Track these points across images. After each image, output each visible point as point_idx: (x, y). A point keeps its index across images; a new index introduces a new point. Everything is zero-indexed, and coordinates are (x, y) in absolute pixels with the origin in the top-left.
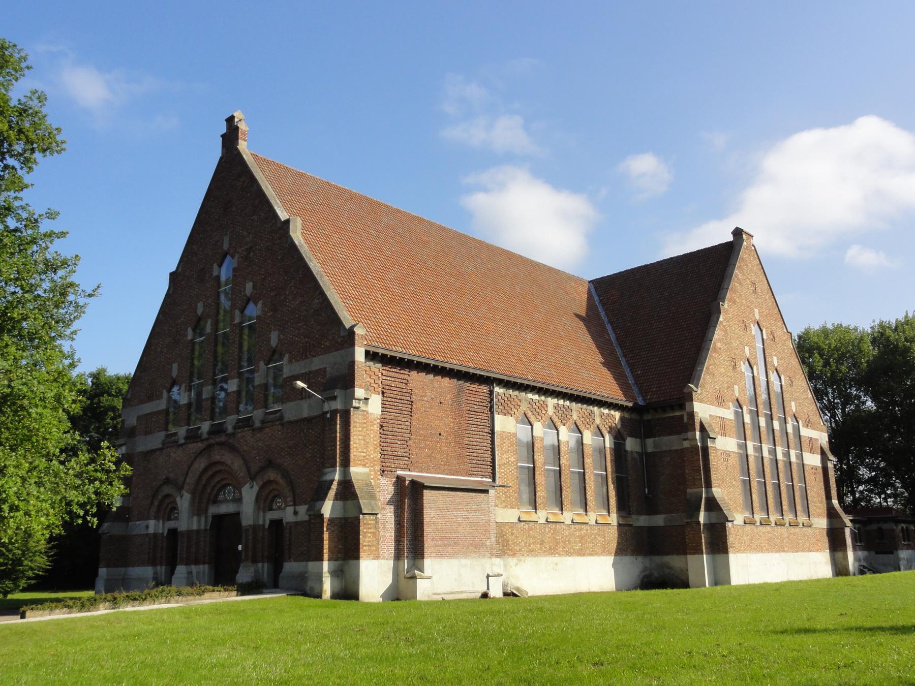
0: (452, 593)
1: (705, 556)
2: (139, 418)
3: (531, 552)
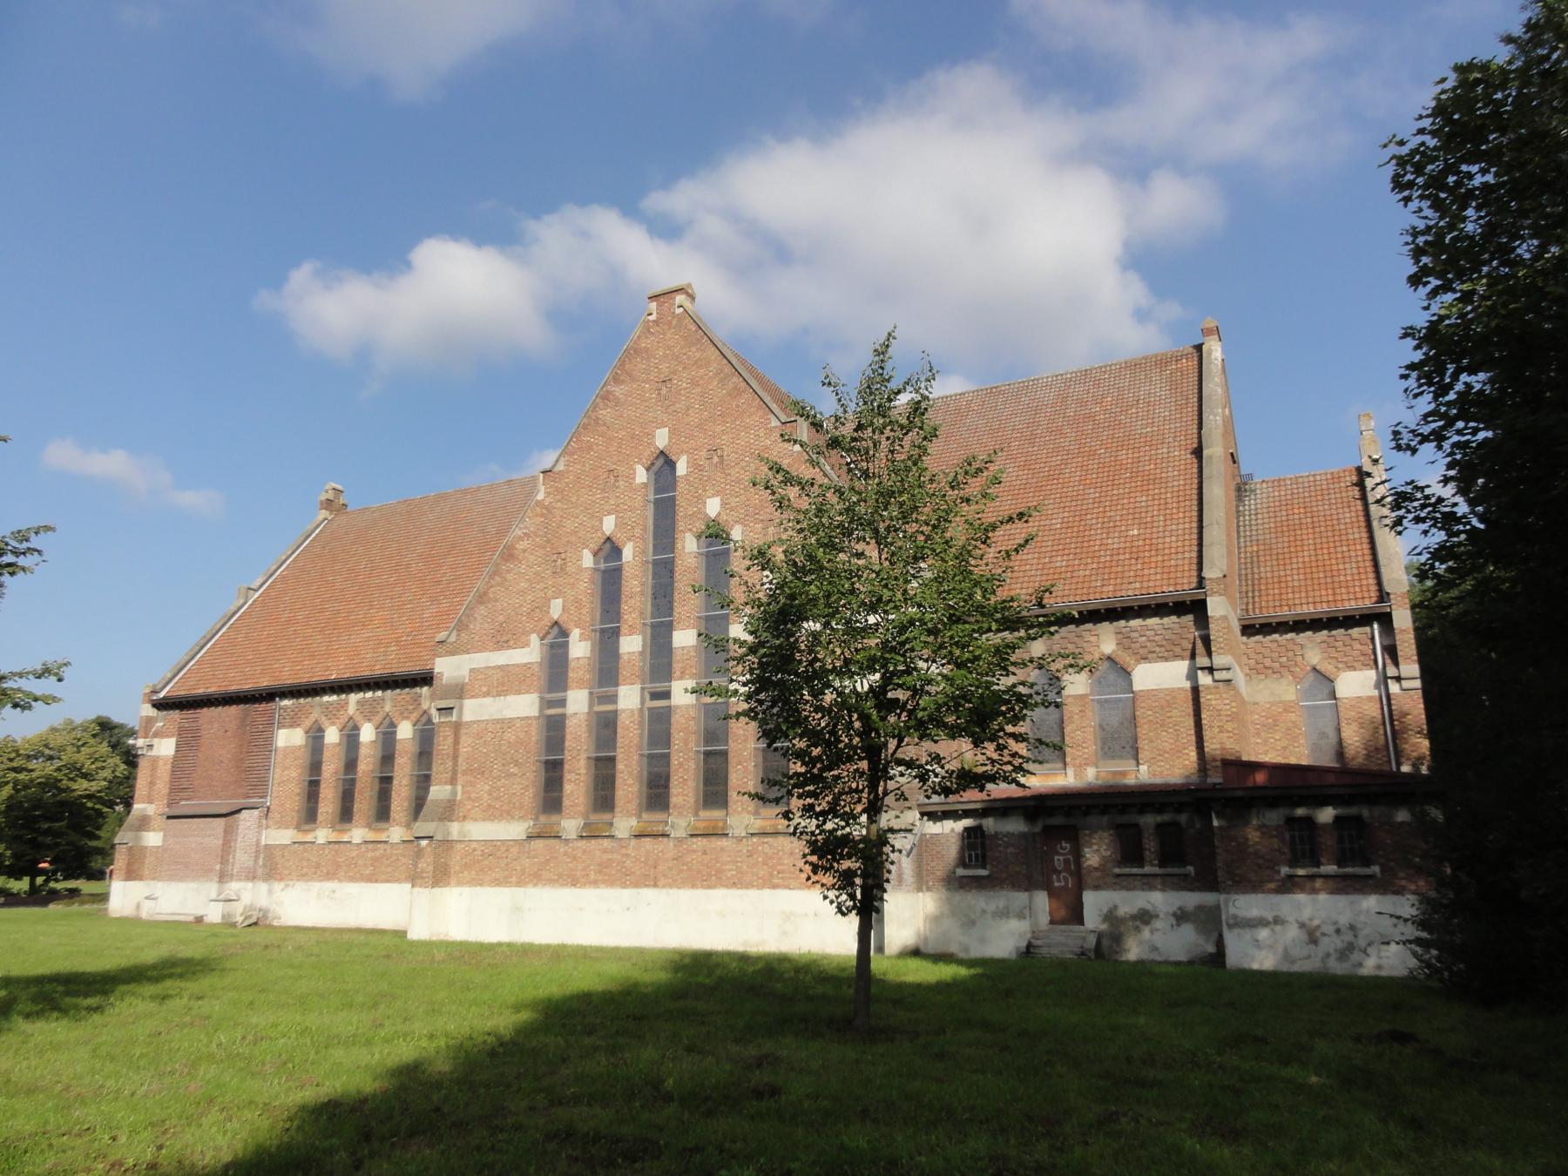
0: (172, 914)
3: (303, 877)
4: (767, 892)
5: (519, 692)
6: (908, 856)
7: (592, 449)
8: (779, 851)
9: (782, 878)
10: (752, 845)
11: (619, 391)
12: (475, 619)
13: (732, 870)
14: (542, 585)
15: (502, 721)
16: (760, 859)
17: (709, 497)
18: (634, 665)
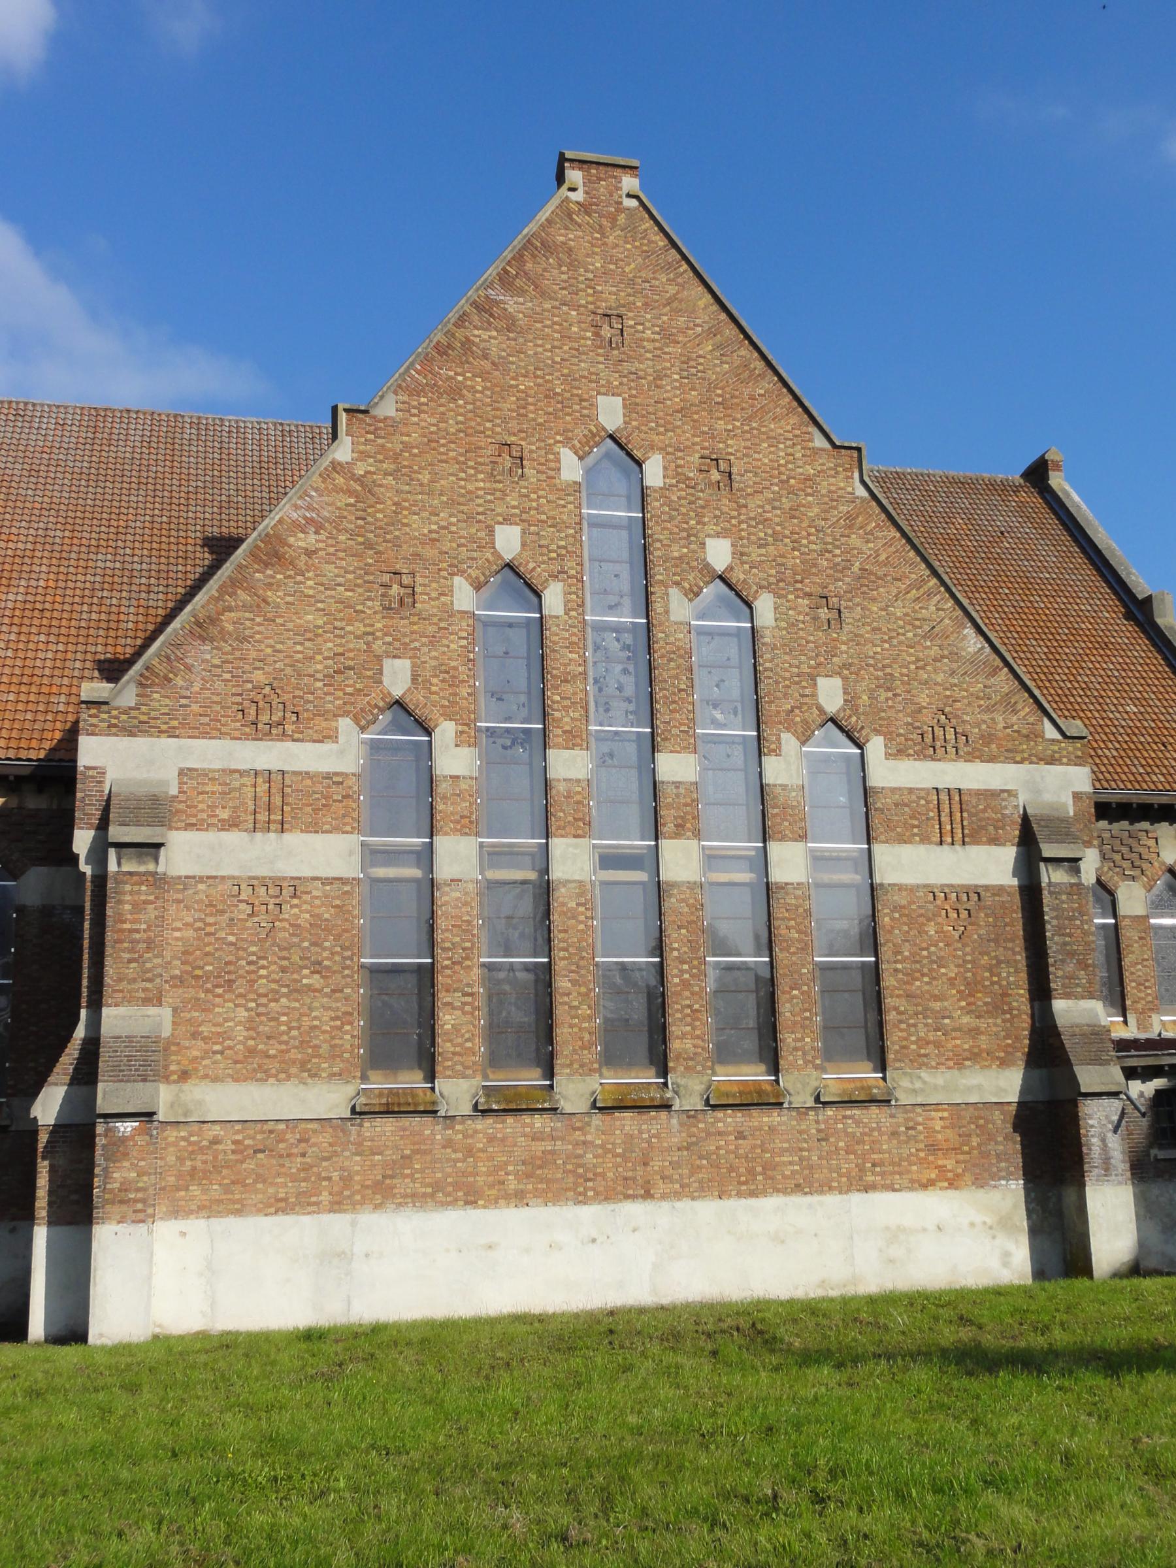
1: (41, 1235)
4: (856, 1198)
5: (314, 828)
6: (1115, 1131)
7: (462, 397)
8: (872, 1129)
9: (883, 1174)
10: (826, 1122)
11: (512, 304)
12: (189, 668)
13: (791, 1163)
14: (359, 628)
15: (277, 883)
16: (841, 1144)
17: (709, 536)
18: (579, 802)
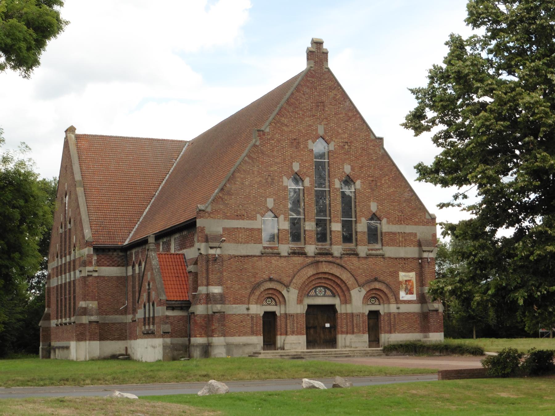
2: (224, 229)
